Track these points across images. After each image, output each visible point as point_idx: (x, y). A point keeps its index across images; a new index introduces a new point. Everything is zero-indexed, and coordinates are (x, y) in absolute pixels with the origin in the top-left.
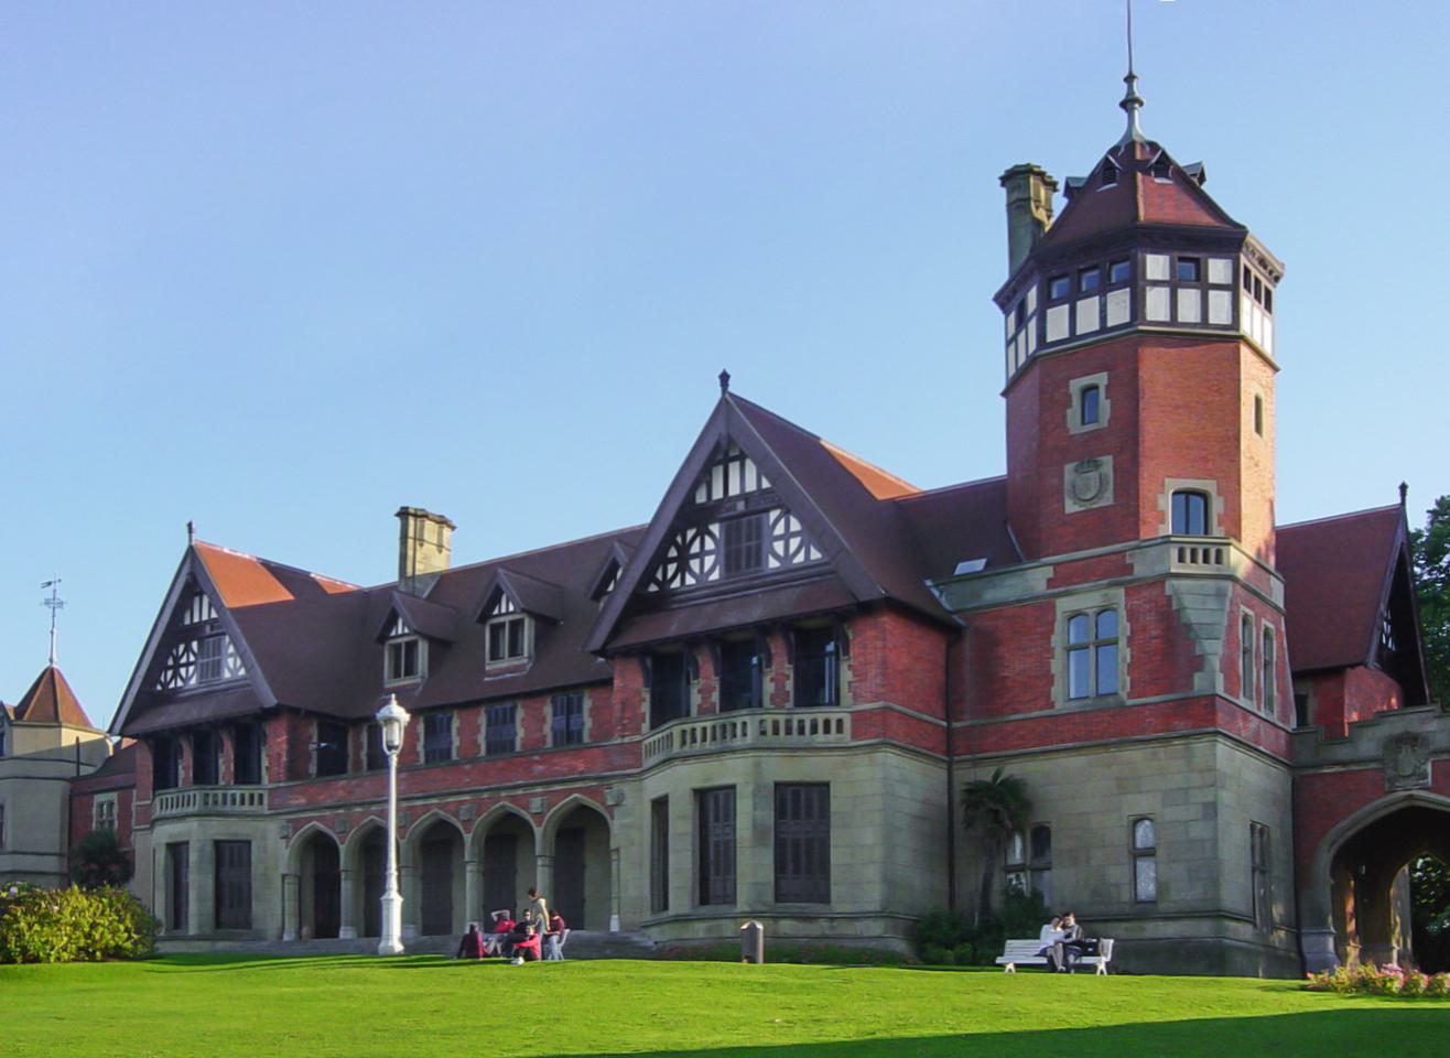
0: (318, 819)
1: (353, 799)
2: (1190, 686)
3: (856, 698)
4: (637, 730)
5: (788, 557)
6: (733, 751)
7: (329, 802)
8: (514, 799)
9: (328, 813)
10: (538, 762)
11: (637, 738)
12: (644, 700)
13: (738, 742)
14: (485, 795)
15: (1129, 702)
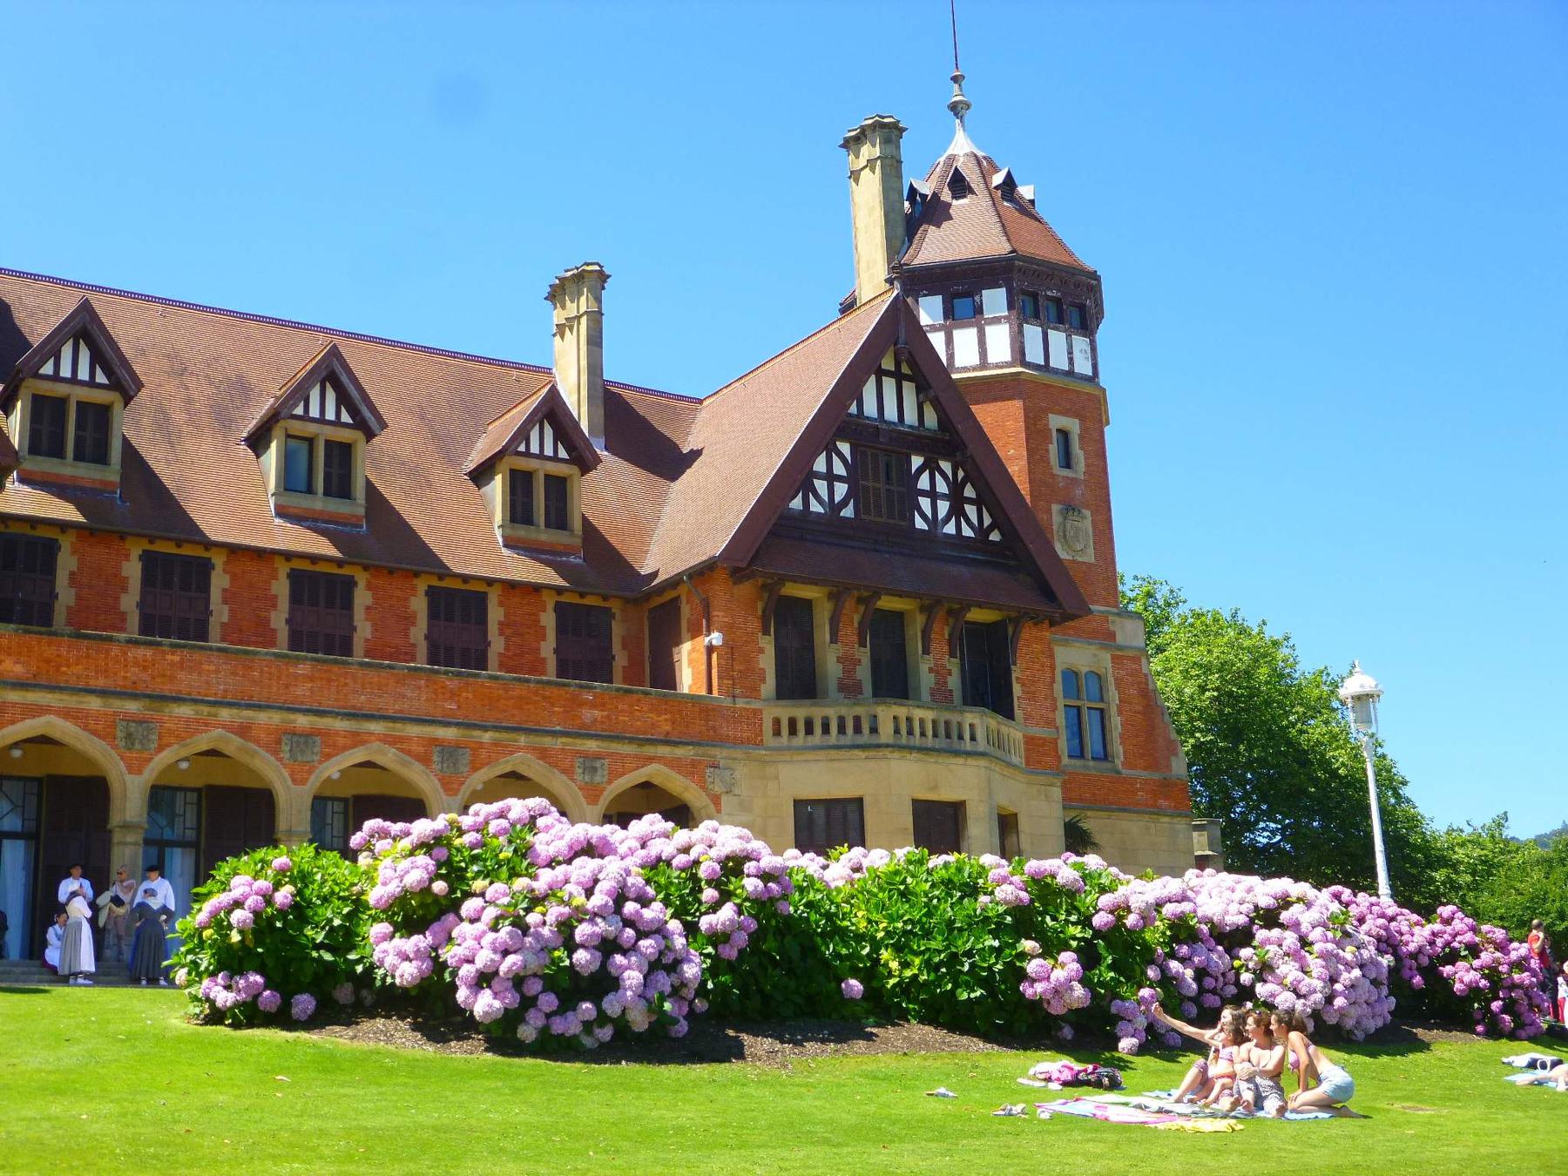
0: (66, 714)
1: (167, 689)
2: (1169, 767)
3: (1028, 717)
4: (753, 692)
5: (933, 522)
6: (969, 754)
7: (101, 683)
8: (543, 754)
9: (94, 703)
10: (593, 706)
11: (755, 705)
12: (761, 651)
13: (968, 745)
14: (487, 737)
15: (1125, 772)
